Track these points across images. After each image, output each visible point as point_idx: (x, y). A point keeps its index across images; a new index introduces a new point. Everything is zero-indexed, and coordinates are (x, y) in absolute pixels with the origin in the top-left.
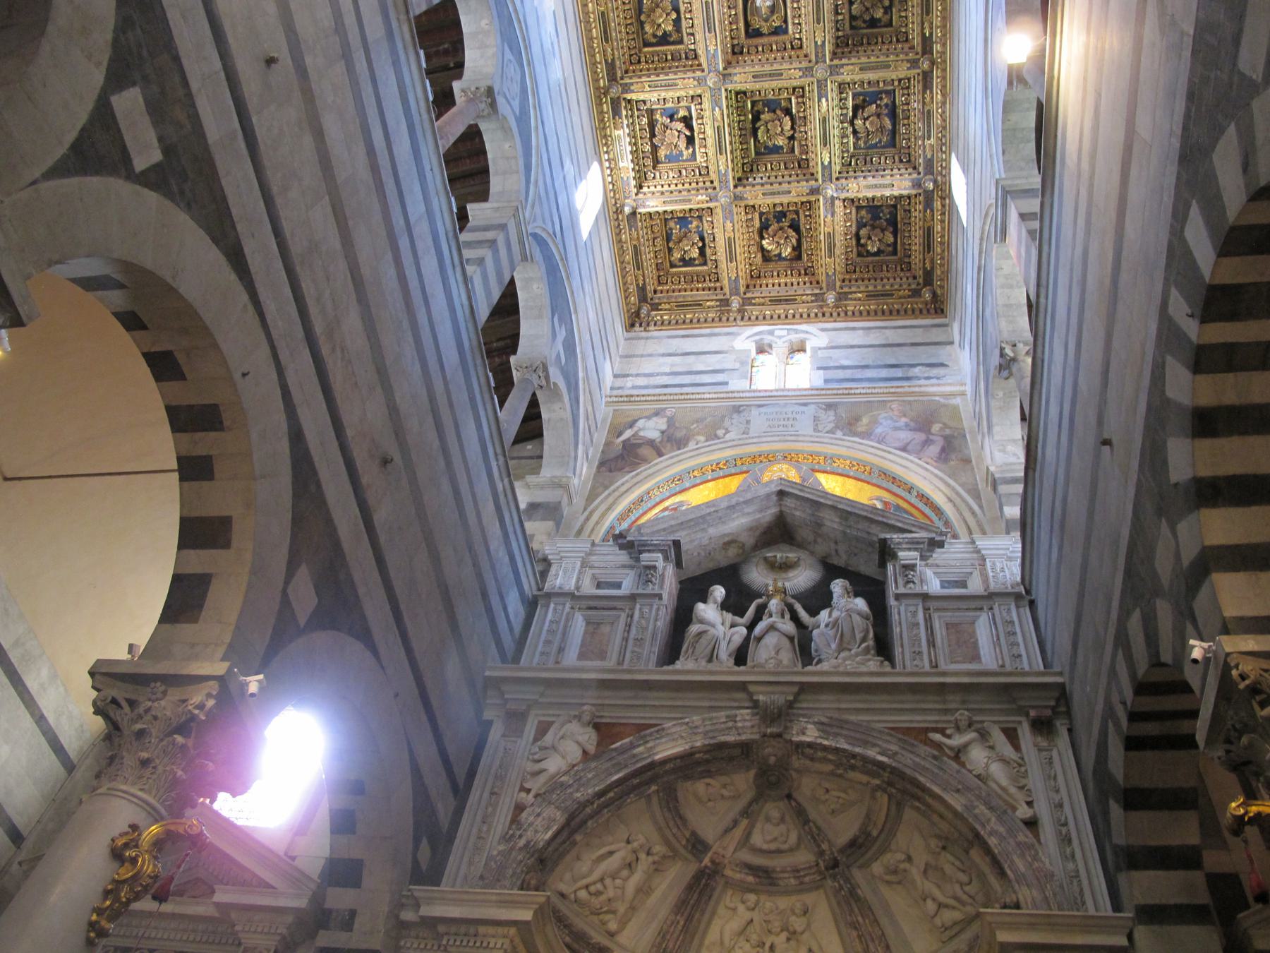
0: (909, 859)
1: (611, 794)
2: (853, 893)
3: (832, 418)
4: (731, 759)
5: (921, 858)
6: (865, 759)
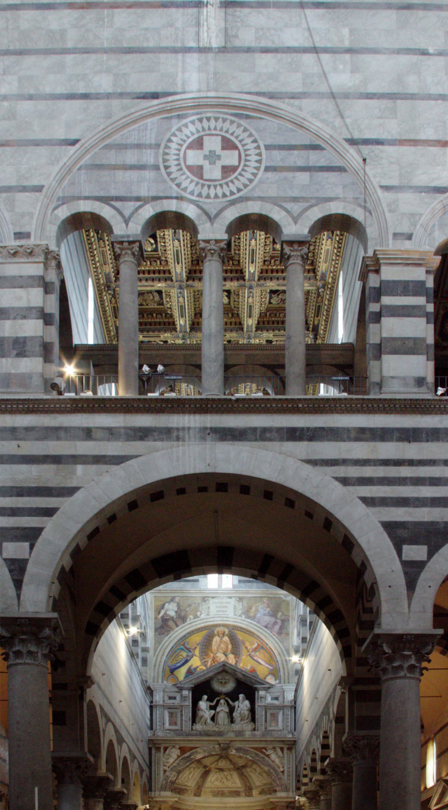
3: (241, 607)
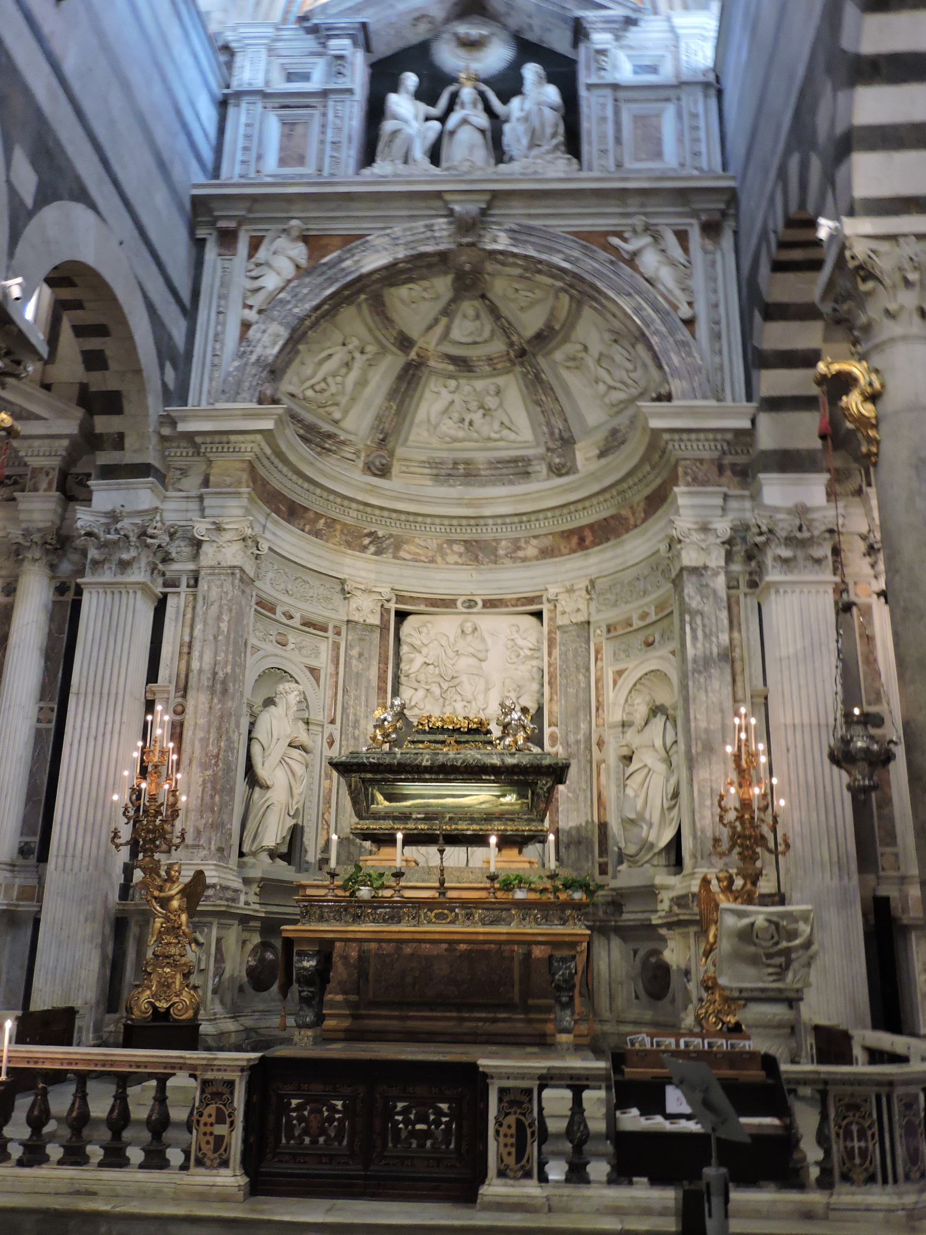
0: (586, 349)
1: (326, 307)
2: (537, 377)
4: (429, 266)
5: (596, 347)
6: (550, 265)
